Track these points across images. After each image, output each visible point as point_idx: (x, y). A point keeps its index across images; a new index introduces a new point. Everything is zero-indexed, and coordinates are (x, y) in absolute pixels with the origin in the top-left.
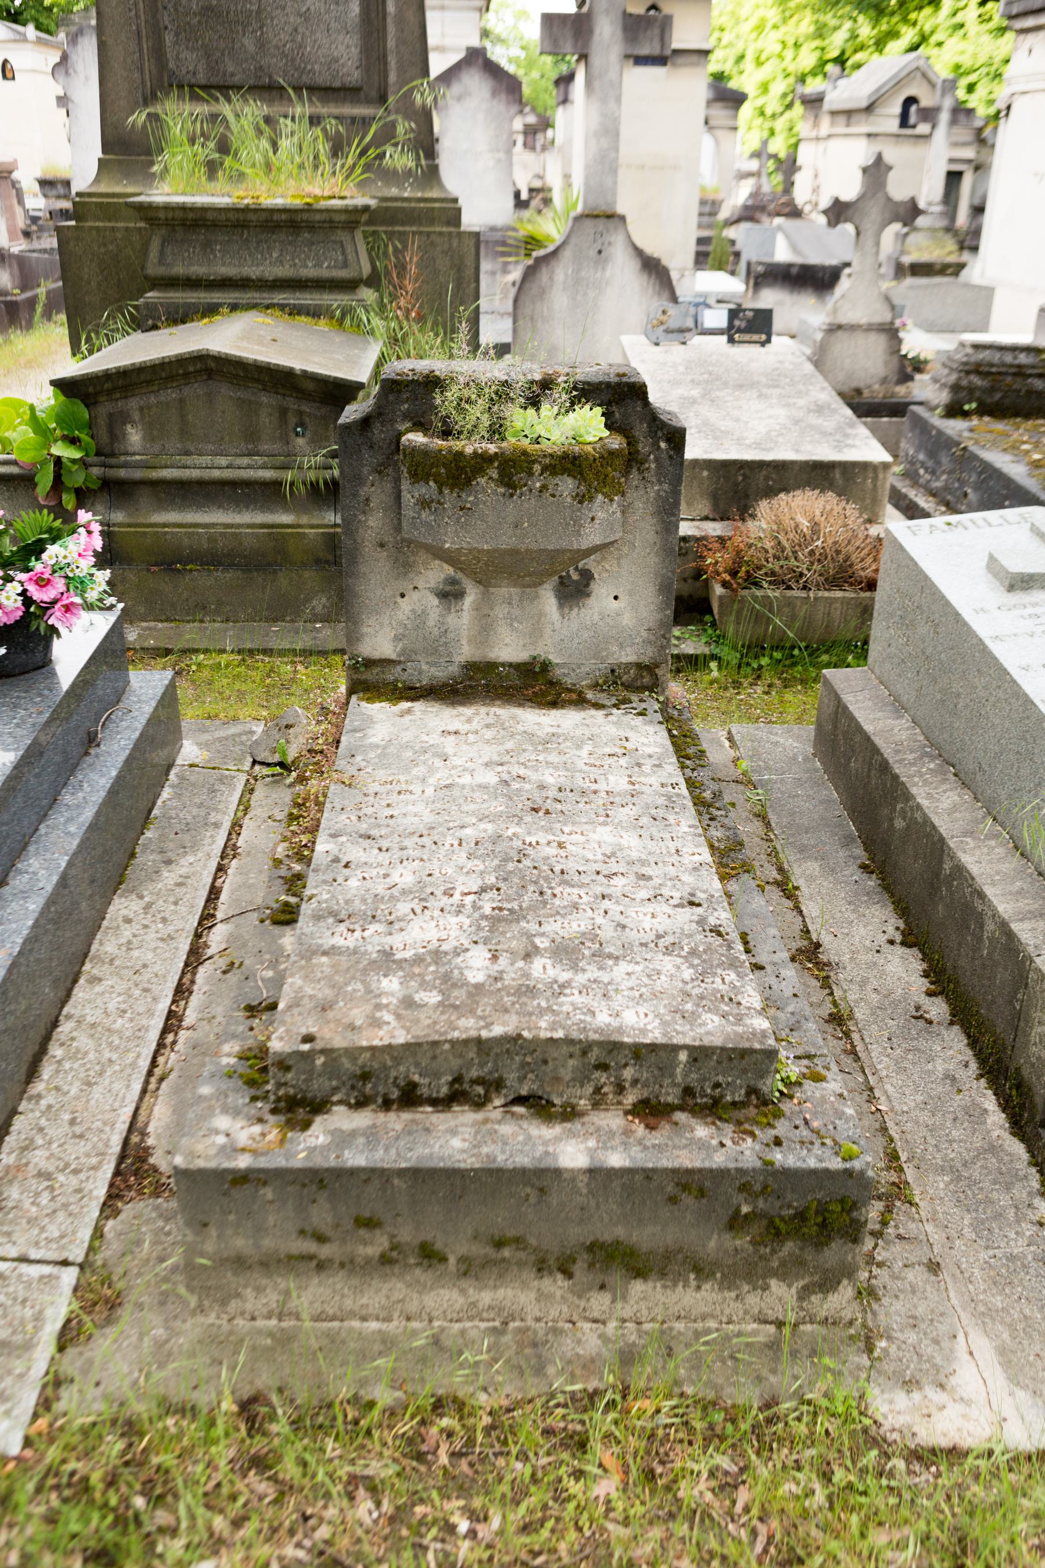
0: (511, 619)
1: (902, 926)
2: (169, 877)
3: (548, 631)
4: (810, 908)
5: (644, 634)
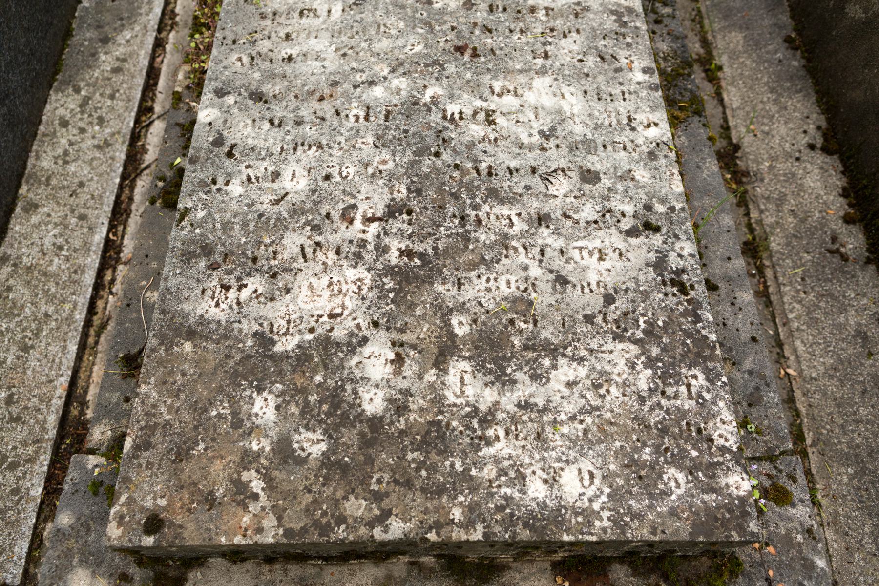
1: (824, 124)
2: (106, 61)
4: (733, 96)
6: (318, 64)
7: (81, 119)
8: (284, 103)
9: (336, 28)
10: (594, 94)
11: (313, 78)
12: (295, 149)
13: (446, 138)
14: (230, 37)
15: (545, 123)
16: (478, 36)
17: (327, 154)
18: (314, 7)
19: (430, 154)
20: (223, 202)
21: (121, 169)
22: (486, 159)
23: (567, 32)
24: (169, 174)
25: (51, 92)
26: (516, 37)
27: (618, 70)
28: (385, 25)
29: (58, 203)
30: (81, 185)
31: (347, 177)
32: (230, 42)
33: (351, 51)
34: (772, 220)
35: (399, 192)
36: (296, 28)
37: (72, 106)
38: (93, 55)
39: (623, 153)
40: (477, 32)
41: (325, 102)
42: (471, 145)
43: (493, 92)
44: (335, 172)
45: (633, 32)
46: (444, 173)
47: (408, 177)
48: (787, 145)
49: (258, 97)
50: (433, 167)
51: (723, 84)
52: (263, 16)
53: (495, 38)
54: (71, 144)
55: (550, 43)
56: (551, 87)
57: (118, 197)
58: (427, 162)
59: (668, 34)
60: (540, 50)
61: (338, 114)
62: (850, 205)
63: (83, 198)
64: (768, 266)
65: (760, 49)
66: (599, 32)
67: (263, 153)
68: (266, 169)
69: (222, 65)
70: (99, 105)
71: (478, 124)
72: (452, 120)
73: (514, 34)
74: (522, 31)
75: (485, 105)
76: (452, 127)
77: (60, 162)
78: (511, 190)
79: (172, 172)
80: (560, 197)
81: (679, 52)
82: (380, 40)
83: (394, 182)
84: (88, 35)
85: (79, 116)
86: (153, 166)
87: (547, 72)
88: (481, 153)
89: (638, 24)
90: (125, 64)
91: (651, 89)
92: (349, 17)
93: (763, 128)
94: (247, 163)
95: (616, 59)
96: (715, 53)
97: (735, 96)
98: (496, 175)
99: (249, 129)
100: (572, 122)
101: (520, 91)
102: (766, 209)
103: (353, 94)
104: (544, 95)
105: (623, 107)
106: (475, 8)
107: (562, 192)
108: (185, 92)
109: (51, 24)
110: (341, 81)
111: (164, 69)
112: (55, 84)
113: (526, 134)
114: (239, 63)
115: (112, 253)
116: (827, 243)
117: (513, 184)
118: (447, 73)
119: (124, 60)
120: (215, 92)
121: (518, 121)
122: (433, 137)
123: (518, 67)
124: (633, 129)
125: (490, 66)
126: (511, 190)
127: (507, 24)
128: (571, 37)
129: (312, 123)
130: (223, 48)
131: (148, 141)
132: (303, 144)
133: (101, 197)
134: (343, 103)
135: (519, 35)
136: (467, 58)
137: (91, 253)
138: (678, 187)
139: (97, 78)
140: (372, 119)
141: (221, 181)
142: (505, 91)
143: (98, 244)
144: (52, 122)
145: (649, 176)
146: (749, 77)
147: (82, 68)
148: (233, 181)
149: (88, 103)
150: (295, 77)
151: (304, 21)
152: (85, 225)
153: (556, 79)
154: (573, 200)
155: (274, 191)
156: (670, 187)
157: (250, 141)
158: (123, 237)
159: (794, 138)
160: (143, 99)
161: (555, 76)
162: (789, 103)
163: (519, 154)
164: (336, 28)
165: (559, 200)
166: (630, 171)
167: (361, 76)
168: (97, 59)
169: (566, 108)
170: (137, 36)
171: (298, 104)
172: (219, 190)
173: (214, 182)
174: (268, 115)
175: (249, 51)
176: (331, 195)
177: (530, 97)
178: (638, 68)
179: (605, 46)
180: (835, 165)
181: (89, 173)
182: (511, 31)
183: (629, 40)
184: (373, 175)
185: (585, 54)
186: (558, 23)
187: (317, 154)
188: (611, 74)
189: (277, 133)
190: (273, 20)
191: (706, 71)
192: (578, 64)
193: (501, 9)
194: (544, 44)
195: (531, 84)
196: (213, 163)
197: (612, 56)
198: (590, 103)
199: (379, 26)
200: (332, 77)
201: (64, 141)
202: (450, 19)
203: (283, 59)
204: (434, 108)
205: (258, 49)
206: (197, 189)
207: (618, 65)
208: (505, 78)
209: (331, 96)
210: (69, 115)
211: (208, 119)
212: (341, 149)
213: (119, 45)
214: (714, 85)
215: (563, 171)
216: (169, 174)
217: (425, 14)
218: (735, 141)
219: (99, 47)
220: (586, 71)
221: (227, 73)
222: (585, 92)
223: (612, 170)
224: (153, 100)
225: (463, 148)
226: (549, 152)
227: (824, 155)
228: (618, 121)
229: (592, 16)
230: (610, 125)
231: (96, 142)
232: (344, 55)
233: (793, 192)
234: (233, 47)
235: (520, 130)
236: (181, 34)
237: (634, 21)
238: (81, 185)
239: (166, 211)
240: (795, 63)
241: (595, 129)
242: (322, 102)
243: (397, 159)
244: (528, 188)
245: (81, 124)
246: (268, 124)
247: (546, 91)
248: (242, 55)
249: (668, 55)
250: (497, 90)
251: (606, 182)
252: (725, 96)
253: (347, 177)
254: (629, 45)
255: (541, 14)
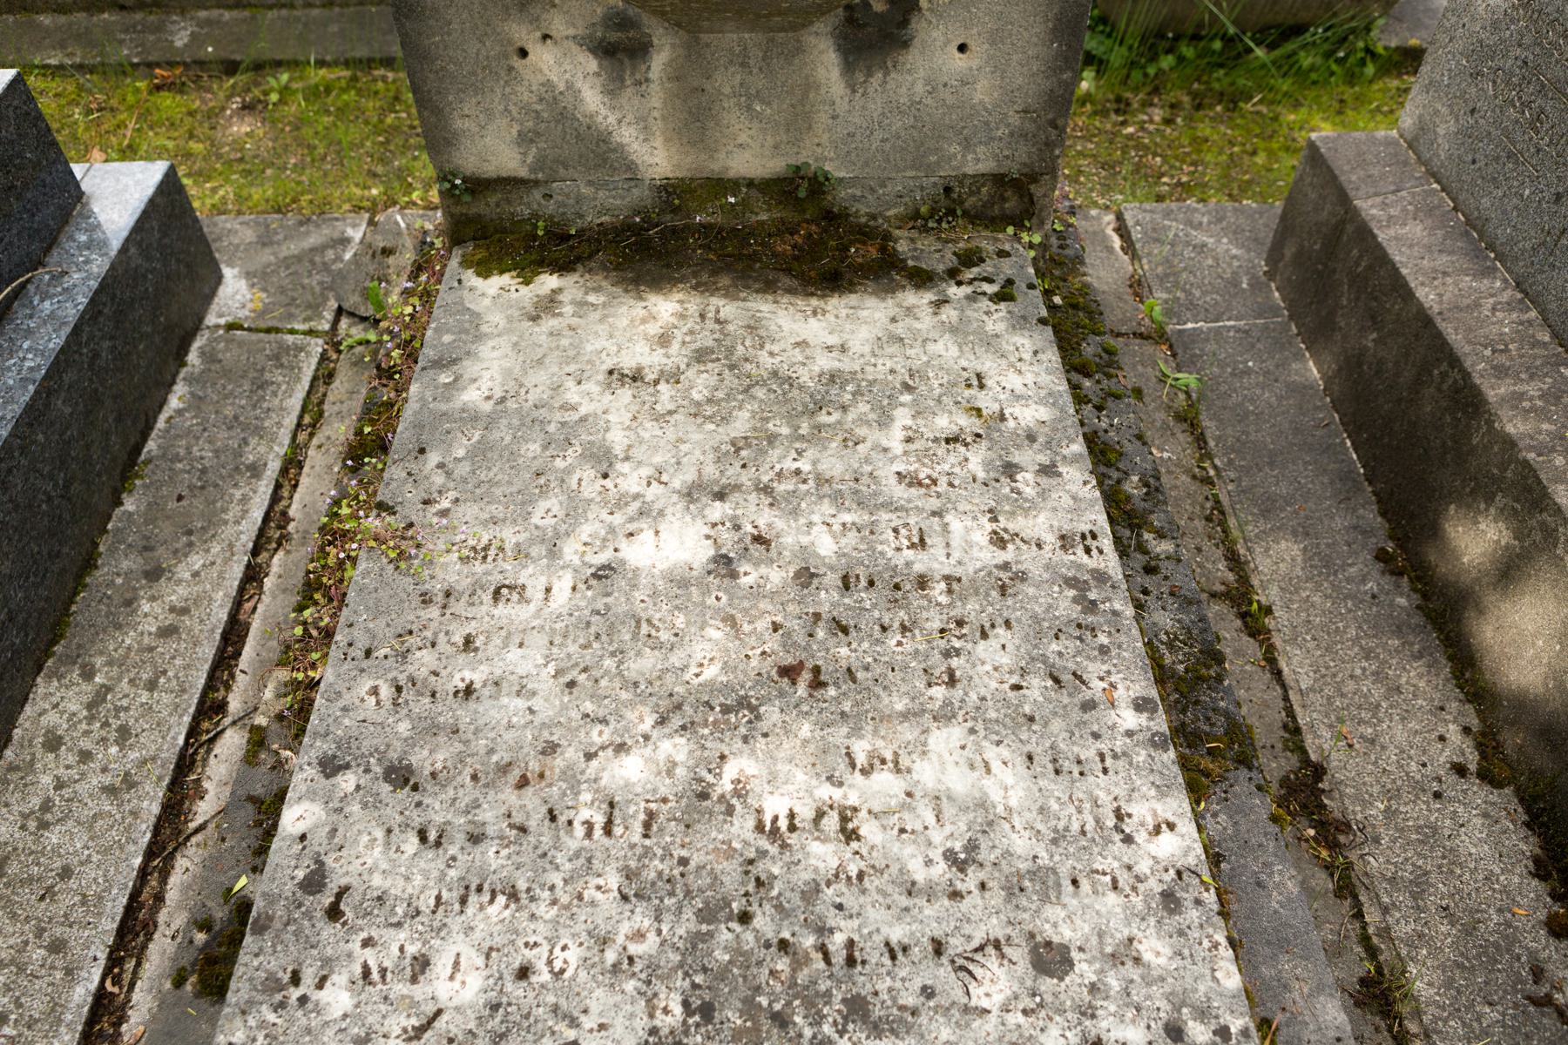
0: (748, 99)
1: (1475, 723)
2: (151, 612)
3: (822, 118)
4: (1297, 665)
5: (1015, 120)
6: (521, 703)
7: (87, 733)
8: (451, 793)
9: (558, 626)
10: (1046, 760)
11: (509, 736)
12: (463, 901)
13: (763, 877)
14: (362, 642)
15: (951, 834)
16: (823, 642)
17: (525, 914)
18: (520, 582)
19: (730, 918)
20: (309, 1031)
21: (149, 835)
22: (842, 924)
23: (987, 625)
24: (220, 914)
25: (39, 680)
26: (894, 642)
27: (1088, 706)
28: (649, 621)
29: (14, 916)
30: (66, 873)
31: (562, 971)
32: (360, 654)
33: (584, 676)
34: (1409, 929)
35: (666, 1011)
36: (485, 627)
37: (73, 707)
38: (128, 603)
39: (1112, 898)
40: (821, 634)
41: (529, 790)
42: (811, 892)
43: (853, 765)
44: (538, 958)
45: (1108, 622)
46: (759, 963)
47: (686, 974)
48: (1414, 766)
49: (401, 776)
50: (737, 951)
51: (1277, 640)
52: (426, 600)
53: (854, 646)
54: (60, 785)
55: (958, 652)
56: (963, 748)
57: (134, 896)
58: (724, 936)
59: (1172, 594)
60: (940, 670)
61: (553, 819)
62: (1555, 896)
63: (66, 901)
64: (1416, 1036)
65: (1335, 574)
66: (1046, 624)
67: (400, 910)
68: (402, 949)
69: (340, 704)
70: (125, 703)
71: (824, 841)
72: (775, 833)
73: (889, 633)
74: (904, 629)
75: (837, 794)
76: (773, 850)
77: (32, 825)
78: (894, 999)
79: (226, 909)
80: (995, 1012)
81: (1195, 632)
82: (639, 654)
83: (658, 986)
84: (125, 565)
85: (84, 726)
86: (211, 826)
87: (954, 717)
88: (833, 911)
89: (1117, 606)
90: (186, 618)
91: (1155, 745)
92: (583, 604)
93: (1362, 729)
94: (364, 935)
95: (1083, 682)
96: (1255, 582)
97: (1301, 665)
98: (864, 962)
99: (378, 850)
100: (1007, 826)
101: (905, 761)
102: (1394, 904)
103: (583, 772)
104: (951, 768)
105: (1104, 789)
106: (815, 581)
107: (998, 999)
108: (275, 726)
109: (58, 554)
110: (563, 742)
111: (256, 625)
112: (50, 663)
113: (921, 859)
114: (373, 700)
115: (105, 1025)
116: (1524, 982)
117: (898, 984)
118: (764, 726)
119: (184, 611)
120: (320, 764)
121: (902, 831)
122: (737, 876)
123: (899, 707)
124: (1128, 840)
125: (847, 706)
126: (894, 999)
127: (876, 614)
128: (997, 636)
129: (502, 838)
130: (346, 667)
131: (208, 771)
132: (479, 889)
133: (101, 898)
134: (564, 794)
135: (899, 637)
136: (802, 690)
137: (63, 1029)
138: (1231, 979)
139: (129, 649)
140: (618, 831)
141: (309, 976)
142: (877, 762)
143: (80, 1007)
144: (30, 741)
145: (1168, 951)
146: (1323, 627)
147: (104, 631)
148: (335, 978)
149: (104, 700)
150: (477, 731)
151: (501, 610)
152: (59, 963)
153: (972, 731)
154: (1021, 1019)
155: (414, 1004)
156: (1214, 979)
157: (377, 880)
158: (132, 985)
159: (1424, 752)
160: (210, 686)
161: (970, 724)
162: (1404, 680)
163: (907, 909)
164: (558, 626)
165: (993, 1019)
166: (1131, 940)
167: (601, 733)
168: (135, 611)
169: (996, 796)
170: (213, 563)
171: (477, 793)
172: (303, 1000)
173: (296, 979)
174: (417, 820)
175: (394, 673)
176: (527, 1016)
177: (925, 773)
178: (1127, 704)
179: (1060, 654)
180: (1511, 807)
181: (86, 847)
182: (884, 629)
183: (1103, 639)
184: (616, 968)
185: (1024, 672)
186: (971, 608)
187: (507, 913)
188: (1076, 715)
189: (432, 862)
190: (444, 607)
191: (1243, 616)
192: (1011, 694)
193: (863, 583)
194: (947, 654)
195: (925, 744)
196: (296, 934)
197: (1074, 674)
198: (1042, 783)
199: (638, 622)
200: (546, 734)
201: (46, 780)
202: (770, 608)
203: (456, 693)
204: (738, 807)
205: (411, 669)
206: (259, 998)
207: (1088, 695)
208: (875, 731)
209: (542, 776)
210: (65, 726)
211: (300, 828)
212: (554, 902)
213: (180, 581)
214: (1261, 643)
215: (997, 945)
216: (220, 914)
217: (724, 599)
218: (1313, 757)
219: (142, 587)
220: (1027, 709)
221: (347, 722)
222: (1030, 758)
223: (1094, 940)
224: (228, 688)
225: (797, 900)
226: (967, 901)
227: (1487, 788)
228: (1097, 821)
229: (1031, 591)
230: (1083, 833)
231: (107, 780)
232: (571, 684)
233: (1440, 867)
234: (365, 664)
235: (909, 850)
236: (294, 556)
237: (1109, 600)
238: (66, 873)
239: (204, 1003)
240: (1402, 601)
241: (1054, 841)
242: (523, 791)
243: (665, 928)
244: (928, 992)
245: (86, 744)
246: (415, 840)
247: (955, 757)
248: (380, 682)
249: (1176, 638)
250: (861, 760)
251: (1085, 970)
252: (1283, 664)
253: (562, 971)
254: (1104, 650)
255: (938, 590)
